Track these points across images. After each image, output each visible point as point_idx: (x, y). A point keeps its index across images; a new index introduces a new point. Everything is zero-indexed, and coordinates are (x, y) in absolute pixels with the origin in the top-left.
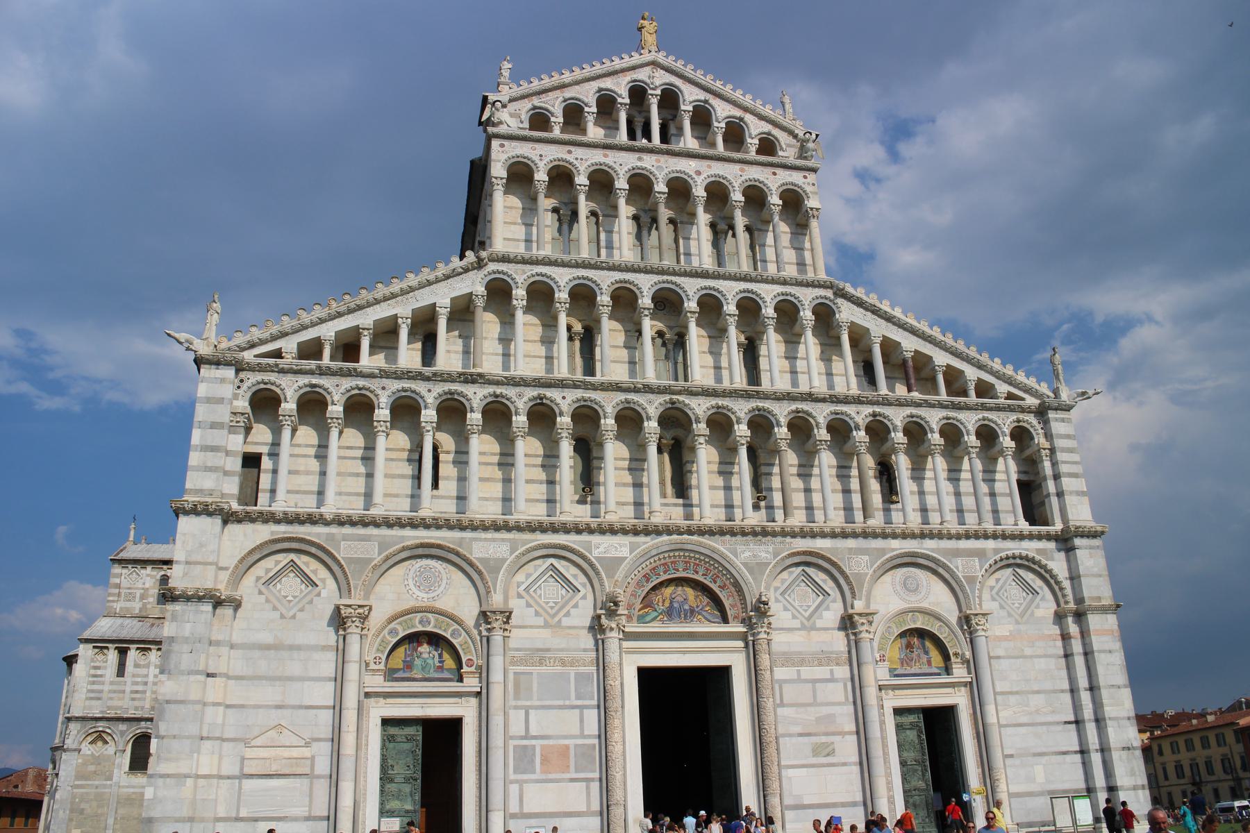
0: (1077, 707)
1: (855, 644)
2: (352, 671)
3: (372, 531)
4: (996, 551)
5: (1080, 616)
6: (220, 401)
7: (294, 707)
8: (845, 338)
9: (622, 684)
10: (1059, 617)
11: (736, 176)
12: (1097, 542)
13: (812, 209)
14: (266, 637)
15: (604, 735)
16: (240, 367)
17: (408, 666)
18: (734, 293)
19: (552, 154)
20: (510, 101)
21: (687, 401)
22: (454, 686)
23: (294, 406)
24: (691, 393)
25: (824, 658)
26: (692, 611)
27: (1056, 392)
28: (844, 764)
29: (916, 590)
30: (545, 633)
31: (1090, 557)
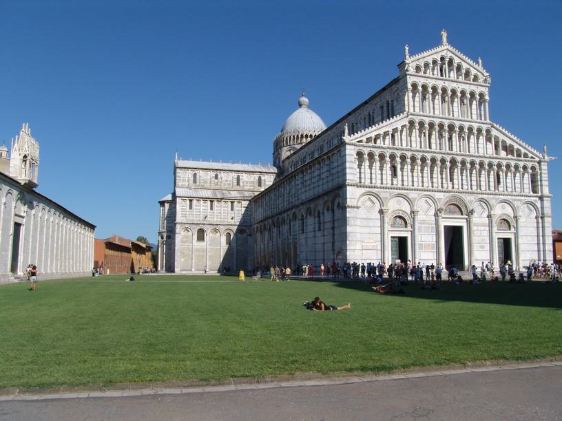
0: (538, 240)
2: (386, 225)
3: (387, 190)
5: (542, 218)
6: (352, 155)
10: (537, 218)
11: (468, 88)
12: (549, 199)
14: (365, 217)
15: (438, 241)
17: (394, 224)
21: (456, 157)
22: (405, 229)
25: (483, 225)
27: (544, 157)
29: (504, 209)
30: (425, 216)
31: (547, 203)
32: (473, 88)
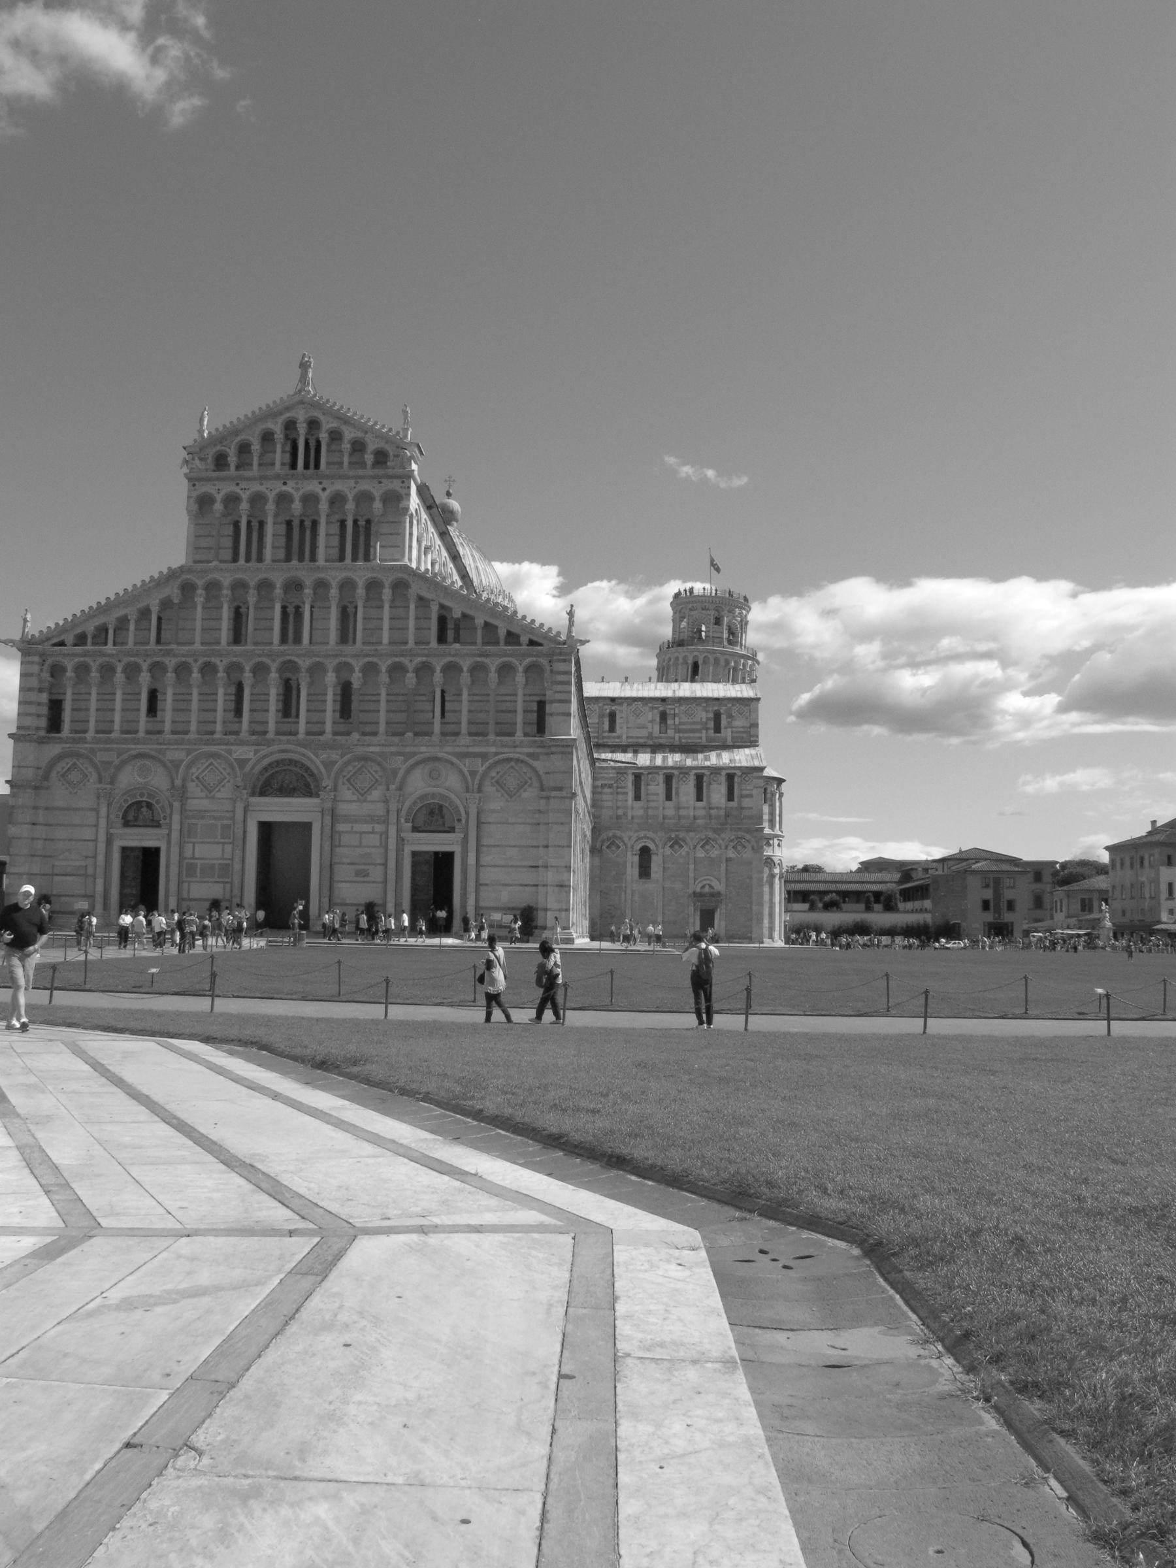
1: (388, 812)
4: (496, 754)
7: (76, 840)
8: (412, 606)
9: (245, 832)
11: (348, 488)
13: (403, 509)
16: (43, 655)
17: (136, 819)
18: (337, 580)
19: (229, 488)
20: (201, 450)
21: (297, 660)
23: (73, 675)
24: (298, 656)
25: (371, 819)
26: (294, 789)
28: (373, 882)
32: (365, 486)
